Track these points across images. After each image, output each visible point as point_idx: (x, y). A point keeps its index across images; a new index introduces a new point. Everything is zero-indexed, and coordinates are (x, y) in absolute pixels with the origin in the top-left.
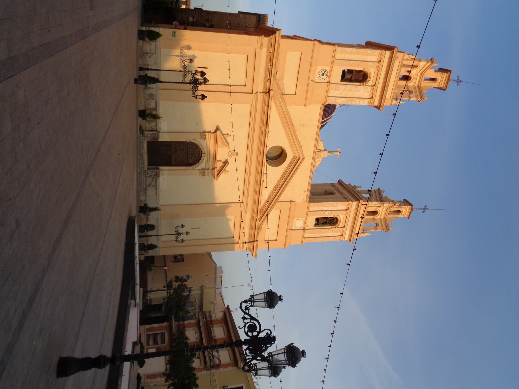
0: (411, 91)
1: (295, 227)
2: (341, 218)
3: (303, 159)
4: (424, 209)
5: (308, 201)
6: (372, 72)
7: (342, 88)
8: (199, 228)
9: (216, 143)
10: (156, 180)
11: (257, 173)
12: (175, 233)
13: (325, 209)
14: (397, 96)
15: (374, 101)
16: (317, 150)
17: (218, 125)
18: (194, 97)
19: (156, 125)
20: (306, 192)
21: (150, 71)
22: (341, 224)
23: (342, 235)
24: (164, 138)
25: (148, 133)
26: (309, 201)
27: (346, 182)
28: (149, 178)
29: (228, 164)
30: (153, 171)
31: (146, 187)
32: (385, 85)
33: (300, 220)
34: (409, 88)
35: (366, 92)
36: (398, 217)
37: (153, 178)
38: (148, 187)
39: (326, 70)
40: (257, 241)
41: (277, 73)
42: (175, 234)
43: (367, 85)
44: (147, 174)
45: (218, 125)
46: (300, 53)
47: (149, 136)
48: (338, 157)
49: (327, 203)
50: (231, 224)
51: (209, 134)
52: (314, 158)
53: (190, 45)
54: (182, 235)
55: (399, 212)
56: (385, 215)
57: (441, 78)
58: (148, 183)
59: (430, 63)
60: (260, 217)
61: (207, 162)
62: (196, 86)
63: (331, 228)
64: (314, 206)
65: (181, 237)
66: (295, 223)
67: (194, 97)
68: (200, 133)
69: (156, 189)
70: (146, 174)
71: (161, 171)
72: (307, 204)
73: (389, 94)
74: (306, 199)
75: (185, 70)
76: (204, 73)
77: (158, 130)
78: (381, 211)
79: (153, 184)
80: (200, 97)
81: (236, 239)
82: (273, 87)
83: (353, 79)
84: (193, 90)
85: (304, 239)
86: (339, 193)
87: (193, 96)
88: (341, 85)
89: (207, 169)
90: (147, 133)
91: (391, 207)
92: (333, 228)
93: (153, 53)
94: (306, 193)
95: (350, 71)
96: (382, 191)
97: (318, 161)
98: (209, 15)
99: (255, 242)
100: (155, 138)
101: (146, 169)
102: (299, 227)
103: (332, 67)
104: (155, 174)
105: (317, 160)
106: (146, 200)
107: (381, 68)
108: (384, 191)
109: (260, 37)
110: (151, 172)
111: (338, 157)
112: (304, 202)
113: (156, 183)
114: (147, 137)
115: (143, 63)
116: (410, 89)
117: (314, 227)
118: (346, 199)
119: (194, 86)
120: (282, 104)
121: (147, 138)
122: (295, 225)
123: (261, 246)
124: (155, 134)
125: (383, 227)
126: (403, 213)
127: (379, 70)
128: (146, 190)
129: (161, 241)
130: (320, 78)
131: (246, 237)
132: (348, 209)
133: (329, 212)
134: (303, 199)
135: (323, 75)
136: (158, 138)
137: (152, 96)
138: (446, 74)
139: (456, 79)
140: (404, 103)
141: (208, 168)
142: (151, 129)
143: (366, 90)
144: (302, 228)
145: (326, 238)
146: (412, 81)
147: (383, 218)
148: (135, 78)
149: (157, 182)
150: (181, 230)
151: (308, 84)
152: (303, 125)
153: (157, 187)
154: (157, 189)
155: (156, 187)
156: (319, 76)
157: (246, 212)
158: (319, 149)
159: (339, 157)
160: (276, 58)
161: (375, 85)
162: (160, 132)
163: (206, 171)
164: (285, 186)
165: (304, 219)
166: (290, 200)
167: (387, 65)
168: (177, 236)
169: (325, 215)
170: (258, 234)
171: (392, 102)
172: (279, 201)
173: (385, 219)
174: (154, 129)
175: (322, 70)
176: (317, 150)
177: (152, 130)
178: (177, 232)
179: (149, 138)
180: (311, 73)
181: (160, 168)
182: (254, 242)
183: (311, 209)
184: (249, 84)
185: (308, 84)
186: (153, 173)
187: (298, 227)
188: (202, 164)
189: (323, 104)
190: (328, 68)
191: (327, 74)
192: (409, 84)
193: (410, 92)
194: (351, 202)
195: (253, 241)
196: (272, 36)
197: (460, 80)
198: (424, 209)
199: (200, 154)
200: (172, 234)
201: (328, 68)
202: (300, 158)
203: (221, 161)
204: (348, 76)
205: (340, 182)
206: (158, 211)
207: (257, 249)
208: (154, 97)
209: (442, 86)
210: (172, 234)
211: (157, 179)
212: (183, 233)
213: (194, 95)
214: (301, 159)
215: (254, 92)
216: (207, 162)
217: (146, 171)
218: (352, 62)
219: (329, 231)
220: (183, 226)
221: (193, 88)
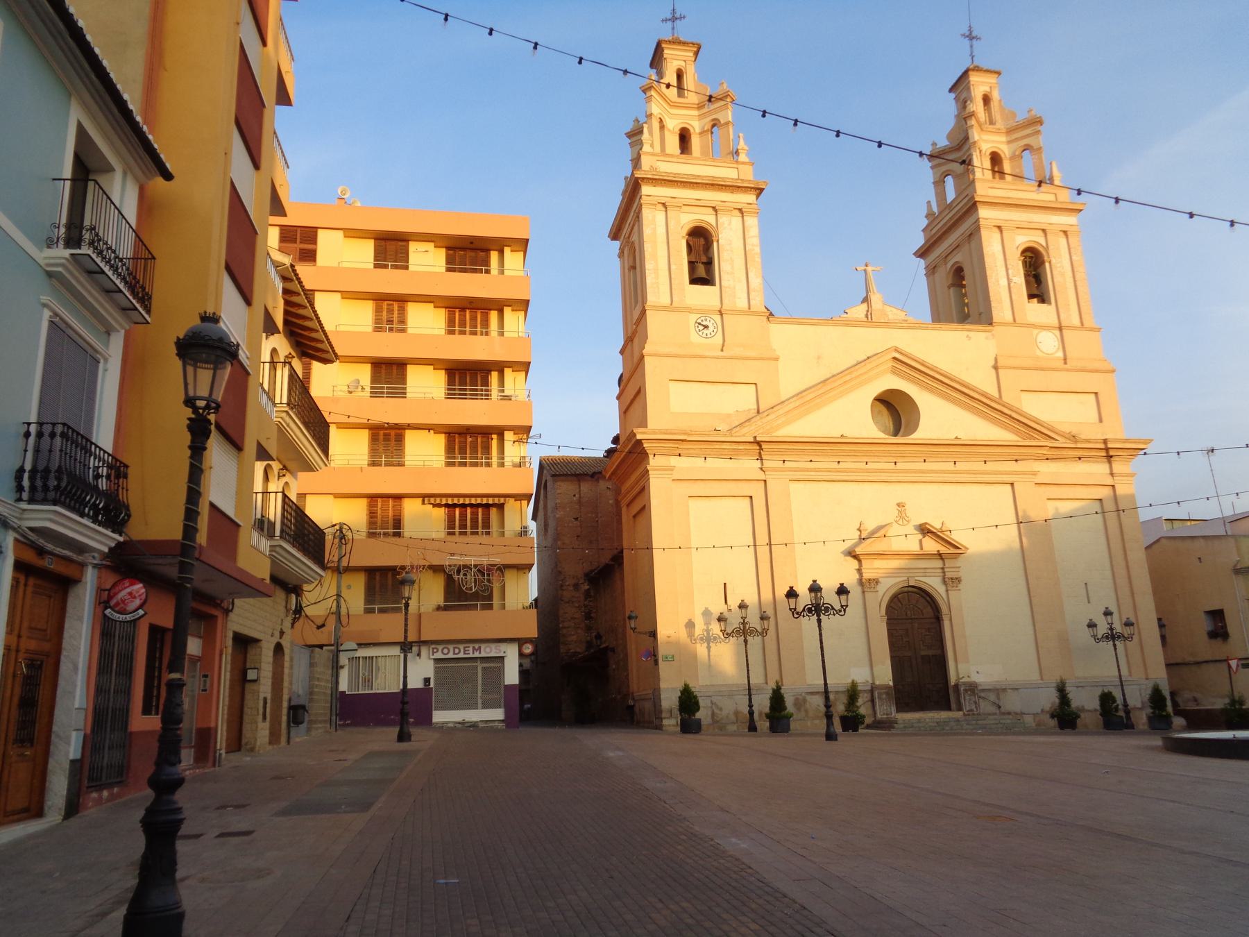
0: (712, 123)
1: (1056, 352)
2: (1023, 240)
3: (897, 350)
4: (971, 37)
5: (990, 328)
6: (687, 220)
7: (729, 280)
8: (1086, 584)
9: (882, 555)
10: (983, 690)
11: (940, 456)
13: (1004, 282)
14: (729, 154)
15: (748, 204)
16: (870, 320)
17: (841, 553)
18: (845, 612)
20: (968, 333)
21: (753, 708)
22: (1037, 239)
23: (1065, 232)
24: (885, 675)
25: (880, 709)
26: (991, 324)
27: (919, 241)
28: (981, 707)
29: (926, 523)
30: (964, 697)
31: (1004, 714)
32: (713, 185)
33: (1038, 341)
34: (706, 129)
35: (729, 224)
36: (1000, 101)
38: (1003, 709)
39: (696, 322)
40: (1105, 441)
41: (717, 429)
42: (1114, 642)
43: (715, 225)
44: (970, 713)
45: (841, 553)
46: (672, 384)
49: (989, 281)
50: (1066, 507)
51: (863, 571)
52: (887, 325)
53: (685, 624)
54: (1113, 626)
55: (986, 100)
56: (998, 132)
57: (675, 59)
58: (993, 709)
59: (653, 93)
61: (928, 574)
62: (823, 608)
63: (1050, 262)
64: (1001, 310)
65: (1118, 628)
66: (1047, 352)
67: (845, 610)
68: (863, 592)
69: (1004, 690)
70: (973, 714)
71: (961, 679)
72: (997, 330)
73: (727, 173)
74: (985, 331)
76: (788, 592)
78: (989, 145)
79: (992, 697)
80: (843, 597)
81: (1104, 493)
82: (747, 435)
83: (704, 259)
84: (832, 613)
85: (1087, 324)
86: (955, 252)
87: (842, 613)
88: (722, 284)
89: (944, 572)
90: (880, 713)
91: (978, 121)
92: (1049, 257)
93: (712, 702)
94: (971, 334)
95: (692, 265)
96: (933, 150)
97: (894, 314)
98: (567, 584)
99: (1110, 445)
100: (887, 694)
102: (1057, 343)
104: (969, 693)
105: (891, 317)
106: (1034, 714)
107: (677, 200)
108: (934, 144)
109: (650, 472)
110: (967, 703)
111: (879, 269)
112: (993, 335)
113: (989, 690)
114: (888, 712)
115: (734, 723)
116: (708, 127)
117: (1050, 303)
118: (974, 234)
119: (823, 612)
120: (781, 412)
123: (1115, 431)
124: (880, 694)
125: (1030, 132)
126: (987, 89)
127: (681, 205)
128: (1009, 713)
129: (1130, 675)
131: (1098, 470)
132: (999, 227)
133: (1010, 271)
134: (987, 338)
135: (706, 327)
136: (887, 687)
137: (799, 703)
138: (666, 51)
139: (669, 24)
140: (741, 135)
141: (941, 571)
142: (870, 703)
143: (726, 225)
144: (1057, 333)
145: (1076, 270)
146: (692, 126)
147: (1007, 136)
148: (824, 738)
149: (987, 687)
150: (1102, 629)
151: (731, 358)
152: (819, 358)
153: (998, 687)
154: (1004, 687)
155: (999, 691)
156: (709, 336)
157: (1034, 474)
158: (867, 316)
160: (689, 435)
161: (714, 208)
162: (873, 683)
163: (948, 575)
164: (964, 385)
165: (1035, 331)
166: (994, 371)
167: (670, 187)
169: (1019, 282)
170: (1088, 441)
171: (744, 163)
172: (998, 397)
173: (1009, 131)
174: (869, 698)
175: (698, 331)
176: (870, 320)
177: (873, 701)
178: (1107, 637)
179: (891, 709)
180: (707, 354)
182: (1107, 449)
183: (1009, 318)
184: (747, 489)
185: (731, 358)
186: (967, 698)
188: (934, 583)
189: (768, 318)
190: (693, 318)
191: (703, 318)
192: (698, 130)
193: (713, 126)
194: (982, 222)
195: (1108, 453)
197: (669, 16)
198: (971, 37)
199: (910, 589)
200: (1115, 649)
201: (693, 318)
202: (895, 358)
203: (921, 541)
204: (701, 271)
205: (922, 253)
206: (1067, 685)
207: (1126, 441)
208: (800, 697)
209: (691, 54)
210: (1115, 649)
211: (980, 688)
212: (1108, 624)
213: (840, 611)
214: (898, 356)
215: (762, 476)
216: (928, 574)
218: (673, 267)
219: (1059, 265)
220: (1092, 625)
221: (827, 614)
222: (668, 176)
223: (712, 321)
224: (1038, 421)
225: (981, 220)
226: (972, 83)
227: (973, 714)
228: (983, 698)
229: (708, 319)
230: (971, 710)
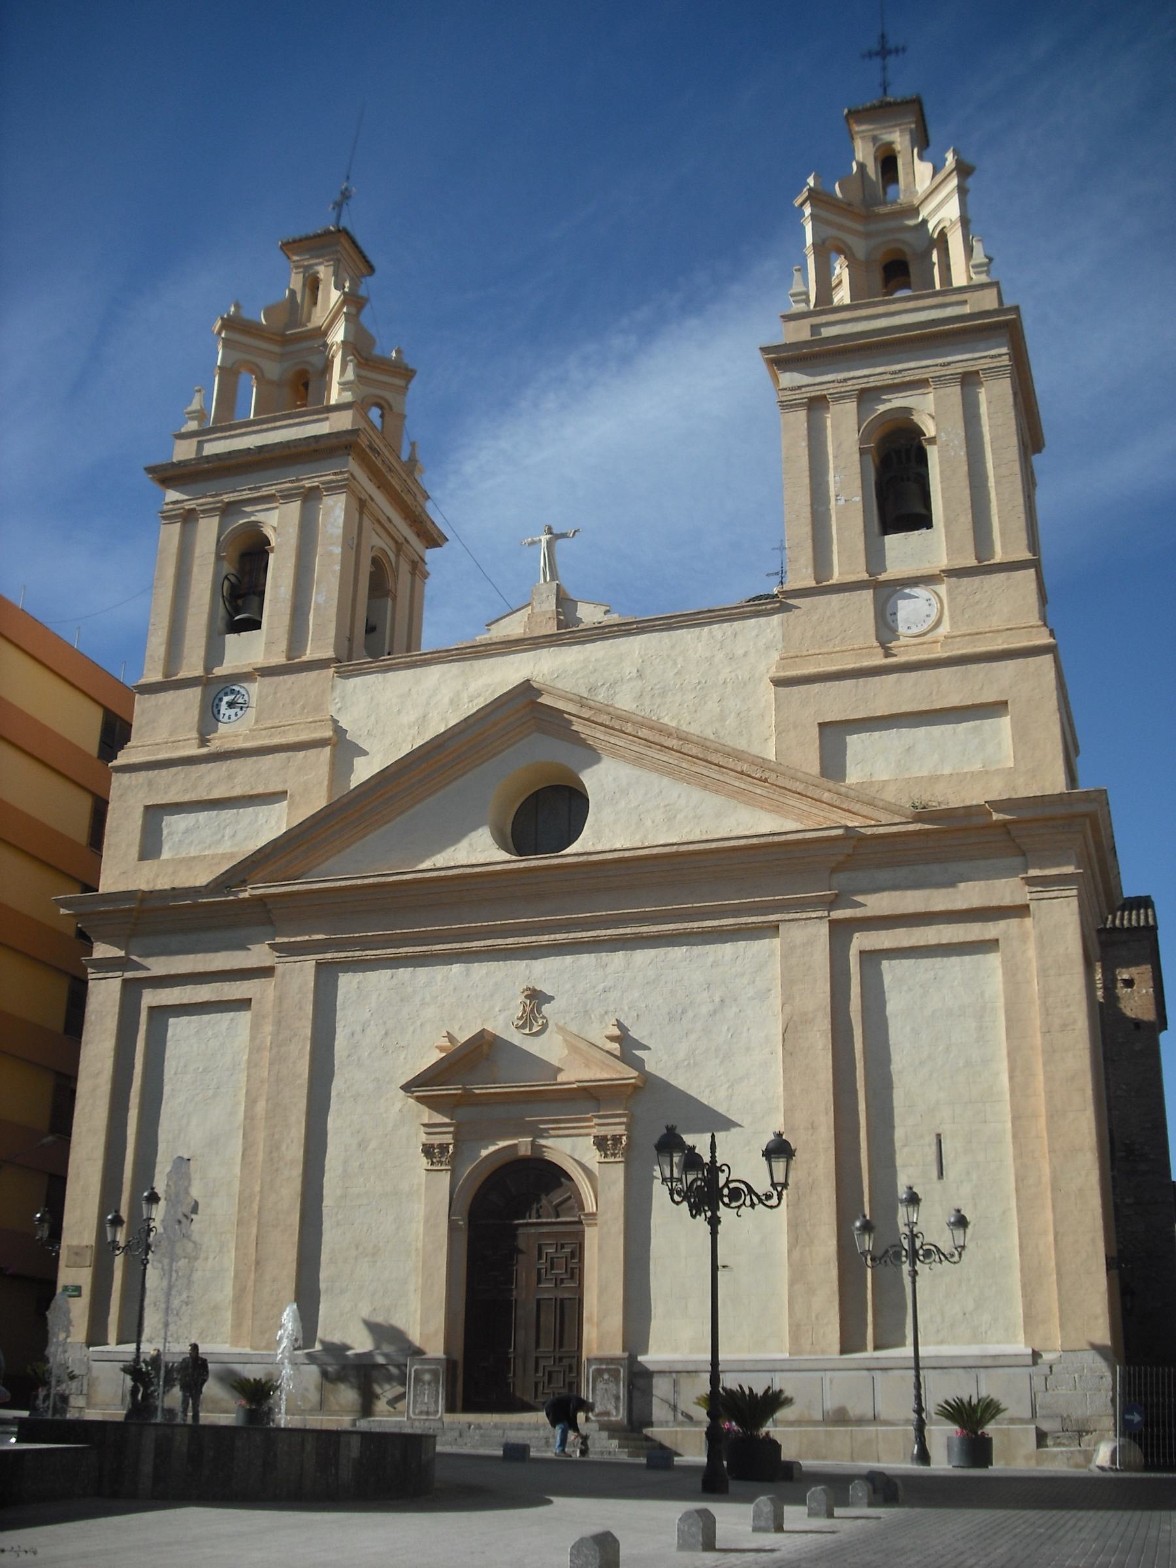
25: (415, 1402)
42: (913, 1264)
54: (915, 1230)
90: (414, 1407)
100: (435, 1373)
104: (606, 1376)
156: (233, 718)
168: (928, 1254)
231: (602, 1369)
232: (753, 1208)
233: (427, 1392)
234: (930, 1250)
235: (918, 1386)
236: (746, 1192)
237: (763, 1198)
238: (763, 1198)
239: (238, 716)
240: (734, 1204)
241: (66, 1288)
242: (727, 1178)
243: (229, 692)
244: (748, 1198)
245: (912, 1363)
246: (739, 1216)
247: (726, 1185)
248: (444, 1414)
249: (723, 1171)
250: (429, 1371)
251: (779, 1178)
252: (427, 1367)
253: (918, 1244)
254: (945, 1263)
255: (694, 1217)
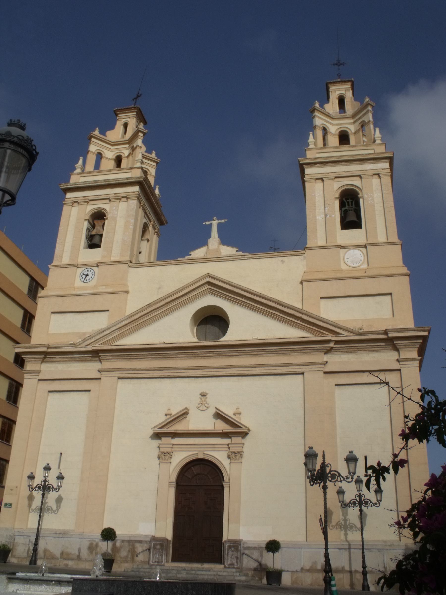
6: (90, 208)
10: (248, 548)
12: (358, 508)
19: (140, 542)
25: (153, 557)
28: (244, 562)
33: (346, 257)
36: (351, 98)
37: (243, 554)
40: (386, 332)
42: (360, 507)
44: (231, 566)
47: (157, 557)
48: (223, 221)
55: (342, 101)
60: (330, 335)
72: (308, 252)
75: (42, 487)
77: (149, 539)
90: (153, 560)
94: (285, 259)
101: (222, 566)
103: (78, 266)
104: (233, 549)
106: (293, 572)
110: (229, 558)
111: (223, 221)
112: (305, 257)
113: (255, 548)
115: (42, 559)
121: (162, 561)
122: (358, 265)
130: (91, 279)
141: (226, 446)
152: (159, 288)
159: (221, 220)
165: (342, 251)
175: (81, 278)
181: (224, 538)
186: (230, 553)
187: (362, 258)
190: (80, 270)
191: (86, 270)
196: (24, 359)
208: (94, 543)
209: (135, 113)
211: (245, 546)
217: (227, 566)
222: (80, 184)
223: (92, 271)
224: (325, 320)
225: (306, 176)
226: (330, 91)
227: (234, 568)
228: (248, 555)
229: (90, 270)
230: (232, 564)
231: (231, 546)
232: (341, 482)
233: (158, 553)
234: (367, 501)
235: (364, 557)
236: (338, 476)
237: (345, 478)
238: (345, 478)
239: (87, 282)
240: (333, 481)
241: (6, 504)
242: (330, 470)
243: (87, 271)
244: (339, 478)
245: (361, 547)
246: (336, 486)
247: (329, 472)
248: (165, 563)
249: (328, 467)
250: (159, 544)
251: (352, 470)
252: (158, 543)
253: (362, 499)
254: (374, 507)
255: (312, 485)
